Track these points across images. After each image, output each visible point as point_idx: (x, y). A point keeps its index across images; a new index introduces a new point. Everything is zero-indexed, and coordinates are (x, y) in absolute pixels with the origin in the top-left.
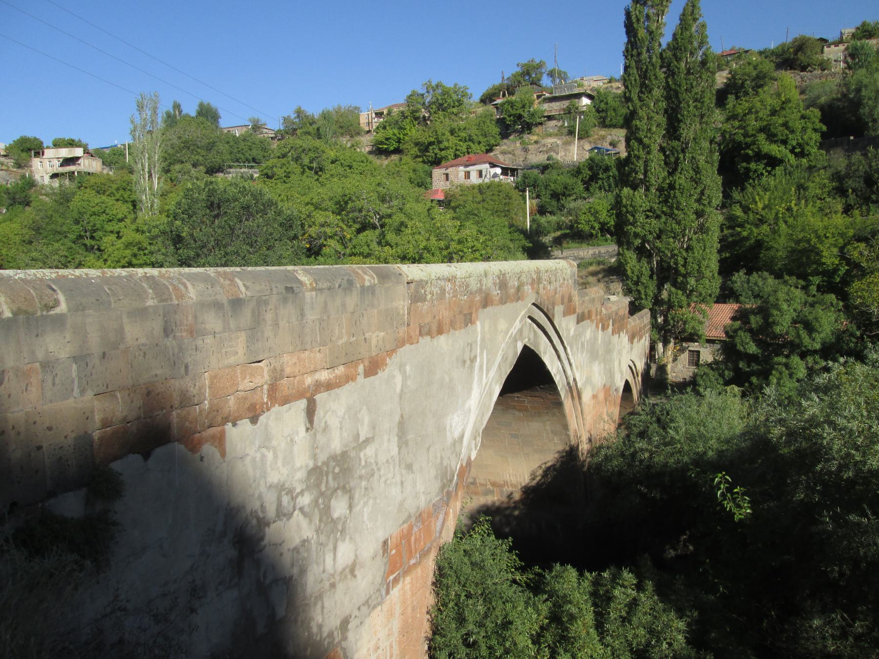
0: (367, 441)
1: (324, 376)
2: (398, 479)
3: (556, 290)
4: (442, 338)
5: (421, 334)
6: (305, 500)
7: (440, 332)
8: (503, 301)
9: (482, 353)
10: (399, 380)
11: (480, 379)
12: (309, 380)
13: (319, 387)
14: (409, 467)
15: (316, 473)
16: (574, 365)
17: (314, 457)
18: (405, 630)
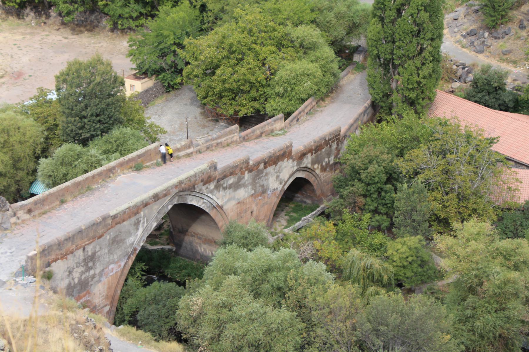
0: (98, 251)
1: (87, 243)
2: (108, 256)
3: (196, 181)
4: (125, 223)
5: (116, 224)
6: (83, 264)
7: (124, 221)
8: (155, 201)
9: (144, 219)
10: (108, 237)
11: (143, 226)
12: (83, 245)
13: (86, 245)
14: (111, 254)
15: (85, 260)
16: (215, 198)
17: (84, 256)
18: (109, 288)
